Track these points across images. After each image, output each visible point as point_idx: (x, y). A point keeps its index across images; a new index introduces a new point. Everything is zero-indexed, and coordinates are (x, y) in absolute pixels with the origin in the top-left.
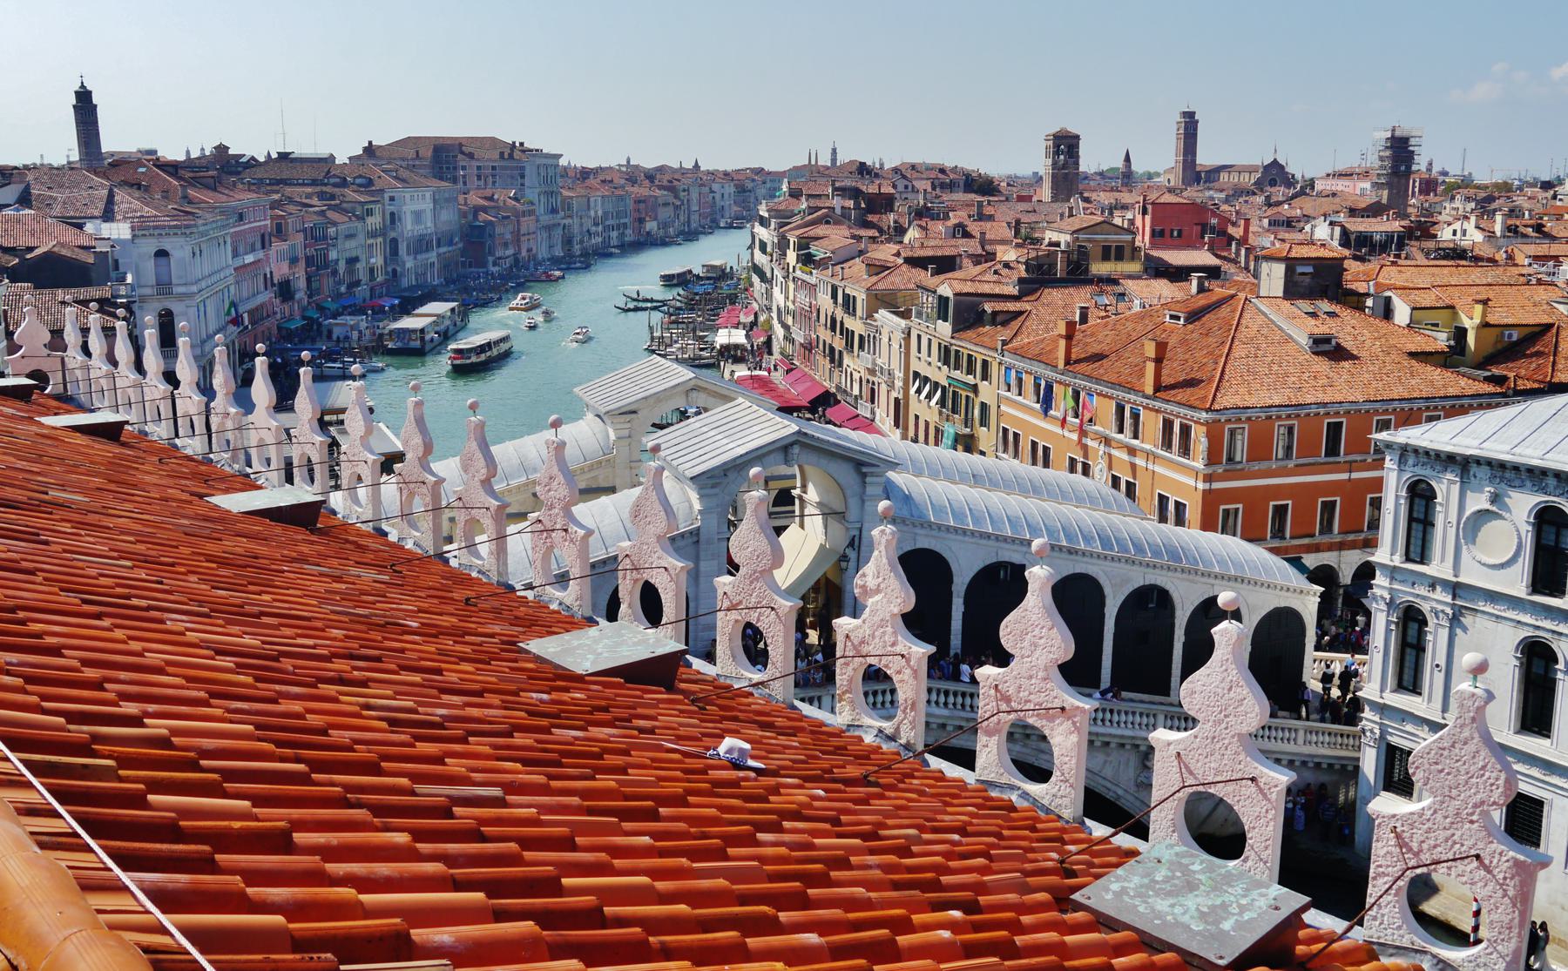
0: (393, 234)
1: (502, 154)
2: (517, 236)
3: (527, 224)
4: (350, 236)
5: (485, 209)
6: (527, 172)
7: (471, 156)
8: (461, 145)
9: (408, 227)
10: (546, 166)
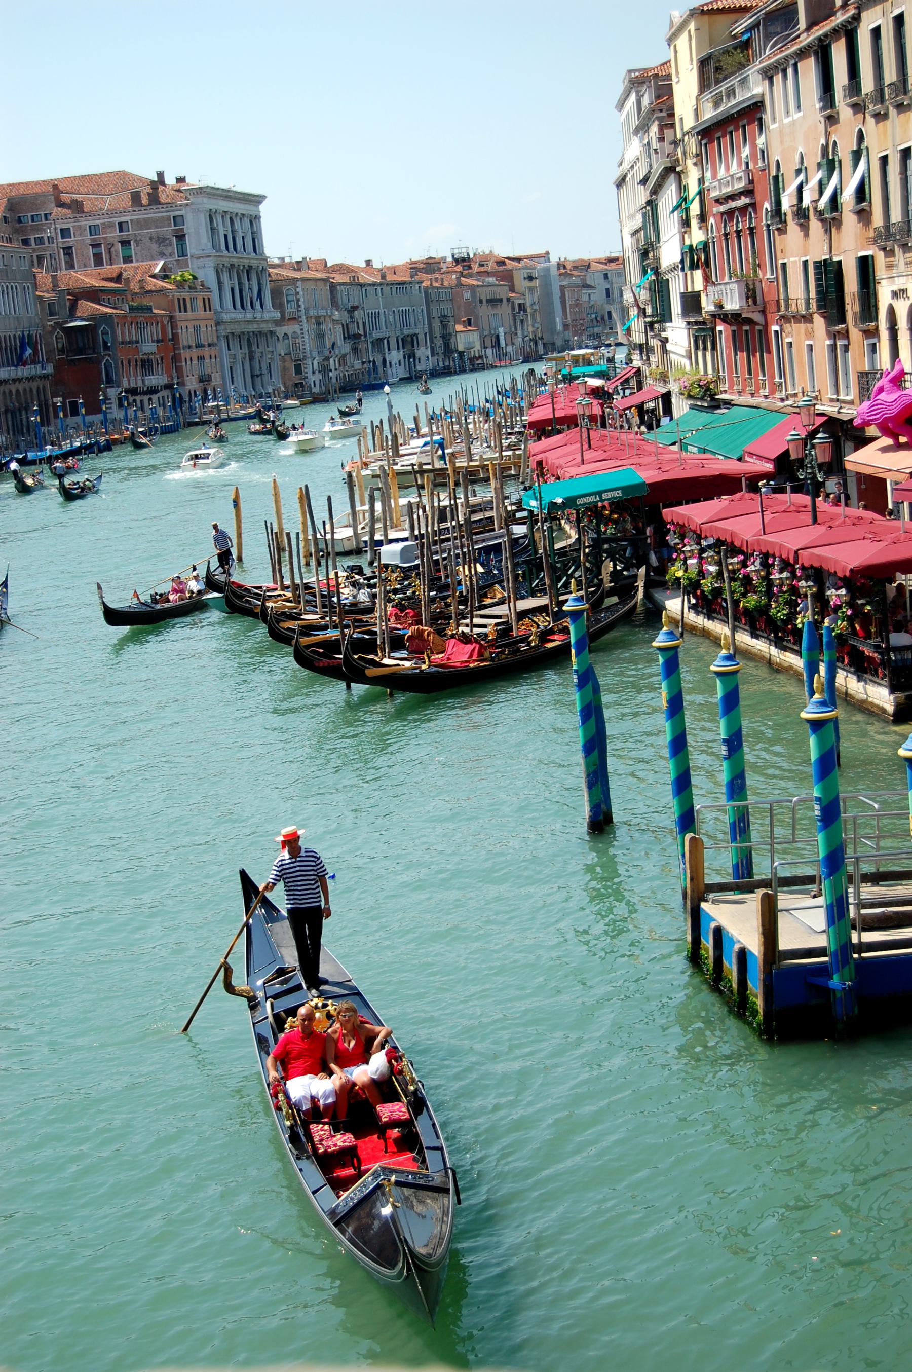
1: (136, 197)
2: (170, 345)
3: (191, 325)
5: (94, 295)
6: (189, 228)
7: (77, 207)
8: (55, 187)
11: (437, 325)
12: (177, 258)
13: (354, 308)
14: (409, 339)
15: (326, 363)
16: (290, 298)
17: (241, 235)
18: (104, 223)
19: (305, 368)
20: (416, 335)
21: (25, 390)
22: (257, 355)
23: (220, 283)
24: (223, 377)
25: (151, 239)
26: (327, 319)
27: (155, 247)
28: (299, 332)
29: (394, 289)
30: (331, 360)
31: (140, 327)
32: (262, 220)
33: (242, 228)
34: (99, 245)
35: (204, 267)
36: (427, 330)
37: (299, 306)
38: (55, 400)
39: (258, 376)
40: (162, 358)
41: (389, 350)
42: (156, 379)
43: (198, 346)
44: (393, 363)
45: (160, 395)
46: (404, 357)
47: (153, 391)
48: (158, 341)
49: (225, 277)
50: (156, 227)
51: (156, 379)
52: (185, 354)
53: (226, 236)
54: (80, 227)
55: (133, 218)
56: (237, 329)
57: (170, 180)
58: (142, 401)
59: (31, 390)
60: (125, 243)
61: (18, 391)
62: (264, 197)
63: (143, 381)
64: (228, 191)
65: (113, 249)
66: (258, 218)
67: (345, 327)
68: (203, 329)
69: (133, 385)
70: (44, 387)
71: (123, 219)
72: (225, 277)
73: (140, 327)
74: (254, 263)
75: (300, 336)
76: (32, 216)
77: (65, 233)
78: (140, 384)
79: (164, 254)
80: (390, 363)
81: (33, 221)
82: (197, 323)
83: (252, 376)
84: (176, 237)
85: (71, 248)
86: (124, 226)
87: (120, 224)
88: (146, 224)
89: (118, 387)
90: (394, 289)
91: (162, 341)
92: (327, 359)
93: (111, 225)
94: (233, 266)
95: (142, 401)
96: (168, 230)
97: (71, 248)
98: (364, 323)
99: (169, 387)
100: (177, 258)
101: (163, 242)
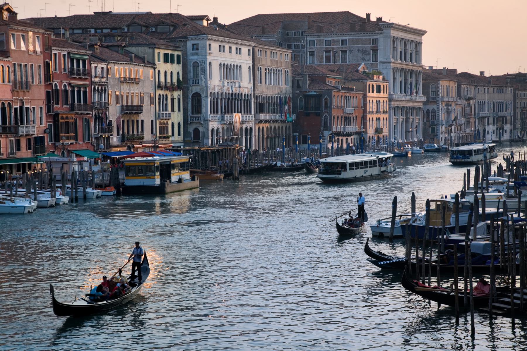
0: (195, 89)
4: (131, 81)
9: (215, 82)
10: (405, 42)
11: (519, 111)
12: (371, 62)
13: (470, 99)
14: (501, 119)
15: (450, 128)
16: (433, 90)
17: (410, 52)
18: (333, 40)
19: (437, 130)
20: (506, 117)
21: (279, 127)
22: (411, 120)
23: (394, 79)
24: (390, 131)
25: (358, 50)
26: (453, 103)
27: (360, 55)
28: (436, 109)
29: (495, 90)
30: (453, 127)
31: (347, 99)
32: (423, 44)
33: (410, 49)
34: (329, 52)
35: (386, 68)
36: (512, 114)
37: (438, 95)
38: (295, 134)
39: (409, 132)
40: (356, 117)
41: (488, 124)
42: (352, 128)
43: (378, 112)
44: (490, 132)
45: (353, 137)
46: (497, 129)
47: (349, 134)
48: (355, 108)
49: (398, 75)
50: (362, 44)
51: (352, 128)
52: (369, 116)
53: (401, 52)
54: (320, 40)
55: (350, 38)
56: (401, 104)
57: (373, 19)
58: (342, 140)
59: (282, 127)
60: (344, 52)
61: (275, 127)
62: (426, 32)
63: (344, 128)
64: (405, 27)
65: (337, 54)
66: (420, 43)
67: (464, 109)
68: (381, 103)
69: (338, 130)
70: (289, 127)
71: (344, 38)
72: (398, 75)
73: (347, 99)
74: (415, 68)
75: (436, 112)
76: (295, 32)
77: (312, 43)
78: (342, 130)
79: (365, 59)
80: (488, 132)
81: (295, 35)
82: (378, 99)
83: (406, 132)
84: (373, 50)
85: (314, 52)
86: (344, 42)
87: (342, 41)
88: (356, 42)
89: (330, 130)
90: (495, 90)
91: (358, 107)
92: (451, 126)
93: (338, 41)
94: (402, 69)
95: (342, 140)
96: (368, 47)
97: (314, 52)
98: (475, 108)
99: (359, 133)
100: (371, 62)
101: (365, 53)
